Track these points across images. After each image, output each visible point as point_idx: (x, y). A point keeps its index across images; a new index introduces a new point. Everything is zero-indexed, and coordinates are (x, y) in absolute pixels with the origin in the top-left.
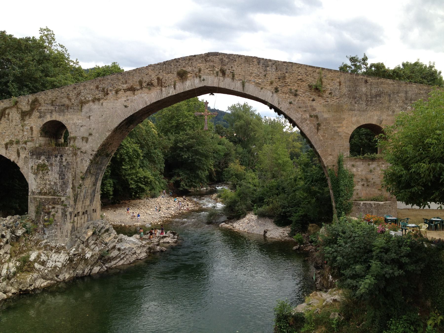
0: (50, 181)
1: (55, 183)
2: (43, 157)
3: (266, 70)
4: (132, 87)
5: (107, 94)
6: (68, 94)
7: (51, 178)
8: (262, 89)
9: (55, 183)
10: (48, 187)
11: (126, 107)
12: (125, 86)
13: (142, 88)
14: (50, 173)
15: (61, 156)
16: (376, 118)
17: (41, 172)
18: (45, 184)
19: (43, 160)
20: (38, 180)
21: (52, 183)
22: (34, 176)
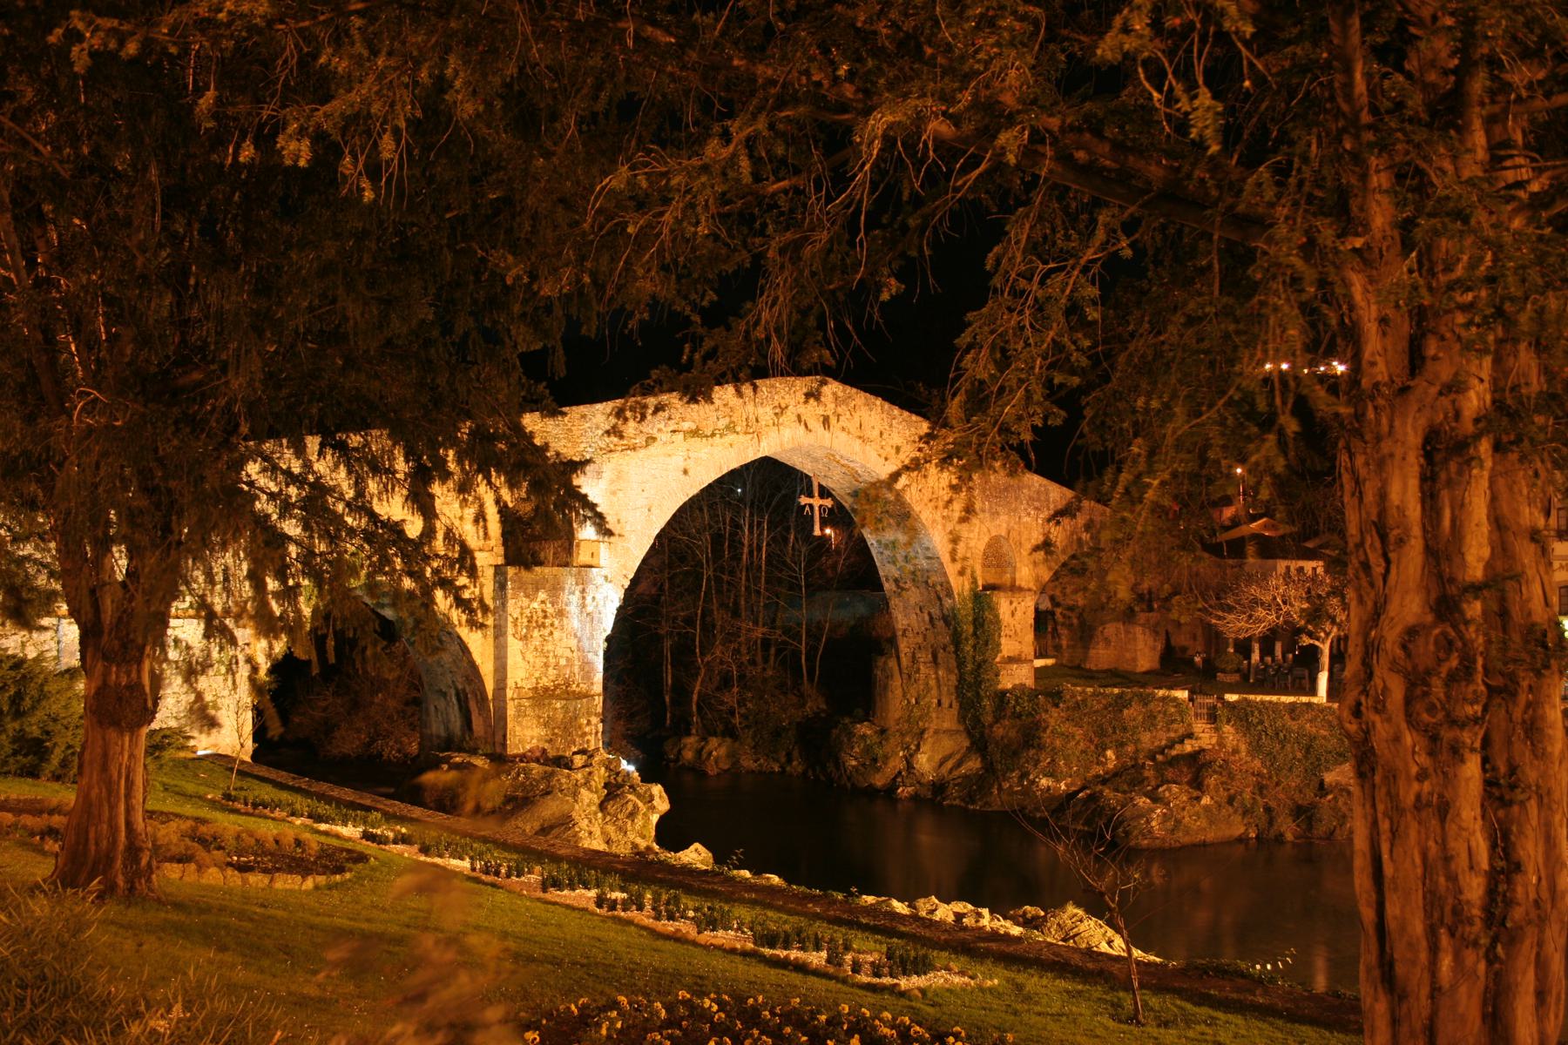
0: (556, 656)
1: (568, 659)
2: (542, 595)
3: (891, 426)
4: (698, 429)
5: (654, 439)
6: (570, 430)
7: (559, 651)
8: (886, 459)
9: (568, 659)
10: (552, 672)
11: (685, 472)
12: (686, 426)
13: (713, 435)
14: (557, 634)
15: (583, 591)
16: (1005, 525)
17: (536, 633)
18: (546, 665)
19: (543, 602)
20: (530, 657)
21: (563, 662)
22: (521, 643)
